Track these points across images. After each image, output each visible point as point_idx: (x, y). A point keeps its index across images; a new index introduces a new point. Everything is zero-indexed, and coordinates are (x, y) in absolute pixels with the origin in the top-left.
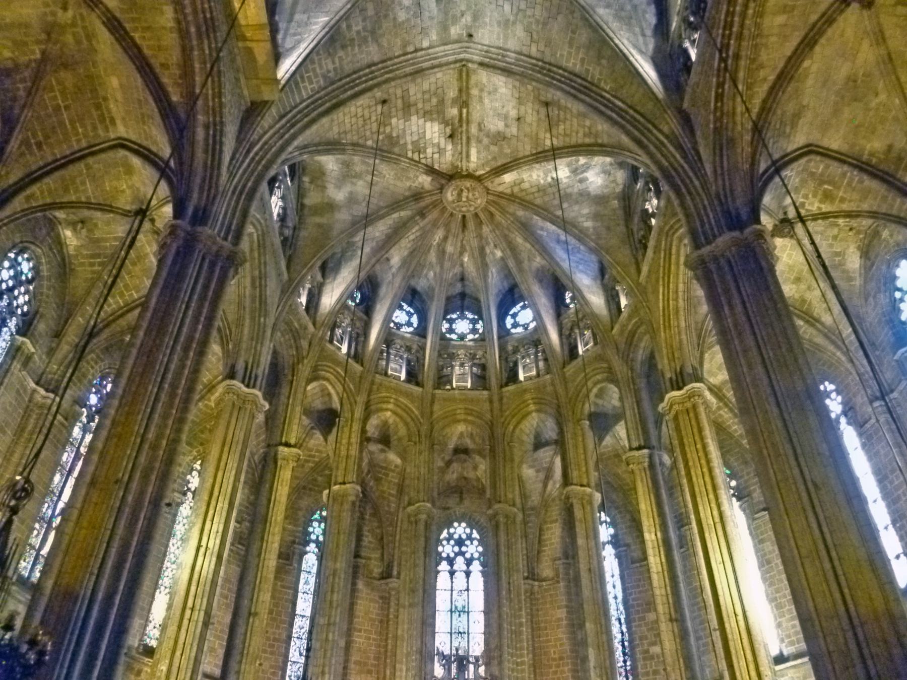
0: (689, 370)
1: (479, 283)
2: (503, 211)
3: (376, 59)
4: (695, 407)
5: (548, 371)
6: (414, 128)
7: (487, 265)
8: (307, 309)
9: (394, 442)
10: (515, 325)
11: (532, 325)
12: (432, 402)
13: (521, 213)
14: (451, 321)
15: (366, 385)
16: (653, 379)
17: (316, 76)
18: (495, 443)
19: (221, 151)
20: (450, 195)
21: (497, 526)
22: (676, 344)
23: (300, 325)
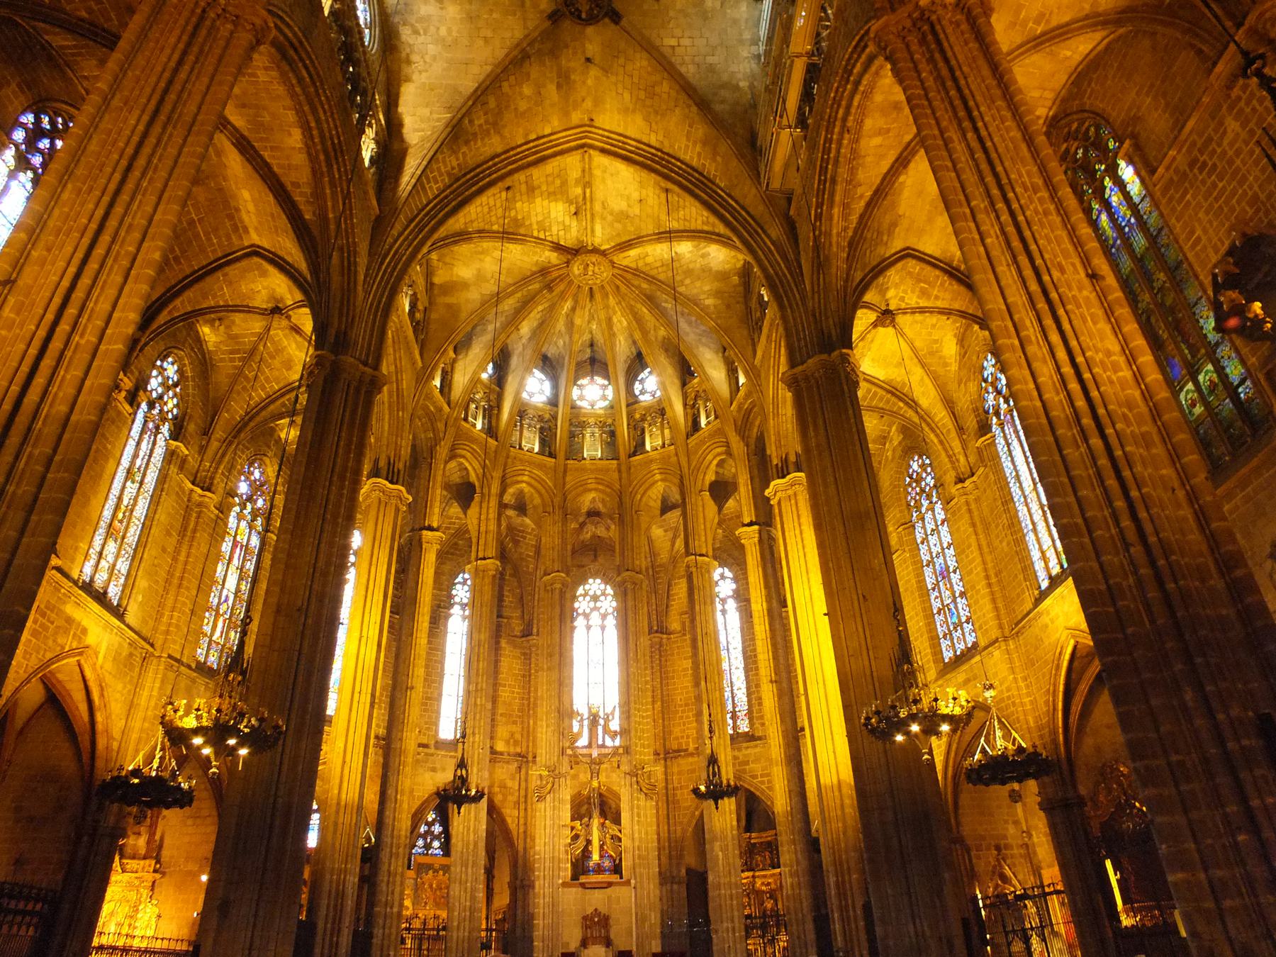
2: (628, 284)
3: (499, 150)
6: (539, 210)
7: (614, 335)
8: (441, 391)
9: (530, 512)
10: (642, 392)
11: (658, 394)
12: (565, 472)
13: (645, 286)
15: (501, 460)
17: (441, 175)
18: (623, 509)
19: (356, 272)
20: (576, 269)
23: (436, 407)
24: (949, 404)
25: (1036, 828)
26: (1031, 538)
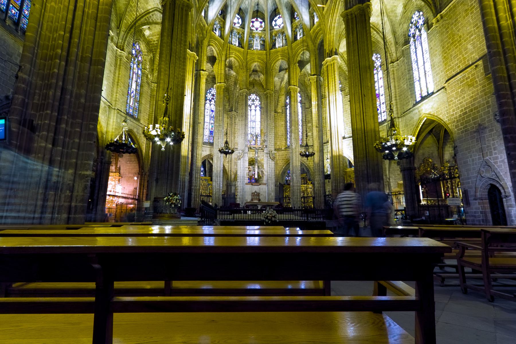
0: (334, 50)
1: (264, 7)
4: (334, 63)
5: (286, 44)
9: (234, 68)
10: (275, 25)
14: (253, 22)
16: (321, 52)
18: (267, 70)
21: (267, 97)
22: (332, 40)
24: (394, 33)
25: (392, 177)
26: (417, 84)
